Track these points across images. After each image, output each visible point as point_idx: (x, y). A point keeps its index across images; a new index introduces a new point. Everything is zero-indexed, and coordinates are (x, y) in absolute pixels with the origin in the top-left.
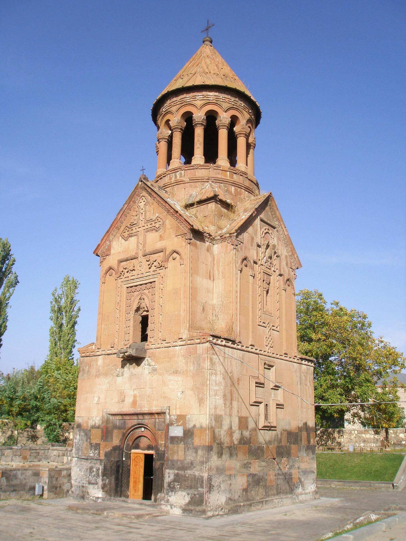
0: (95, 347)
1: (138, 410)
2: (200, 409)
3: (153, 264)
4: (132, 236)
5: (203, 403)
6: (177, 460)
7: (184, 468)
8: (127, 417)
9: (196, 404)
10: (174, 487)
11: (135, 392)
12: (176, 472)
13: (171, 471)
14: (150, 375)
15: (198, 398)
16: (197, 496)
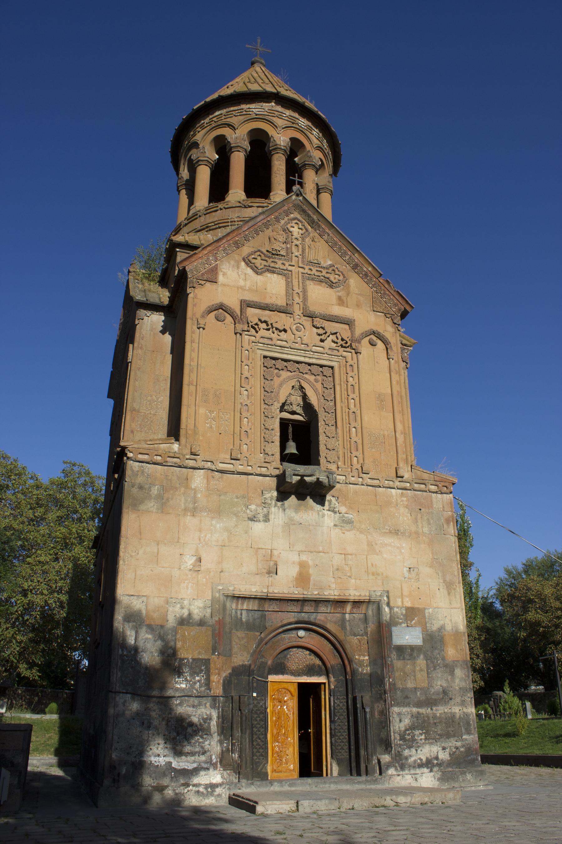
0: (179, 449)
1: (313, 593)
2: (450, 600)
3: (329, 336)
4: (273, 272)
5: (455, 589)
6: (415, 688)
7: (430, 703)
8: (274, 606)
9: (441, 590)
10: (413, 740)
11: (304, 558)
12: (415, 710)
13: (404, 710)
14: (337, 530)
15: (445, 581)
16: (462, 749)
